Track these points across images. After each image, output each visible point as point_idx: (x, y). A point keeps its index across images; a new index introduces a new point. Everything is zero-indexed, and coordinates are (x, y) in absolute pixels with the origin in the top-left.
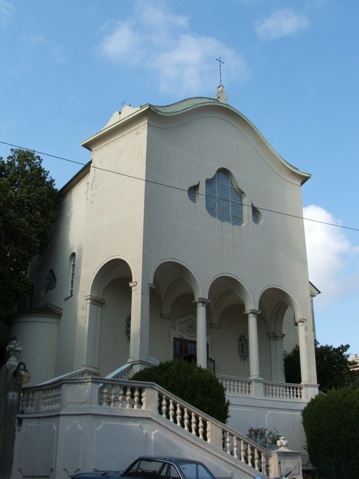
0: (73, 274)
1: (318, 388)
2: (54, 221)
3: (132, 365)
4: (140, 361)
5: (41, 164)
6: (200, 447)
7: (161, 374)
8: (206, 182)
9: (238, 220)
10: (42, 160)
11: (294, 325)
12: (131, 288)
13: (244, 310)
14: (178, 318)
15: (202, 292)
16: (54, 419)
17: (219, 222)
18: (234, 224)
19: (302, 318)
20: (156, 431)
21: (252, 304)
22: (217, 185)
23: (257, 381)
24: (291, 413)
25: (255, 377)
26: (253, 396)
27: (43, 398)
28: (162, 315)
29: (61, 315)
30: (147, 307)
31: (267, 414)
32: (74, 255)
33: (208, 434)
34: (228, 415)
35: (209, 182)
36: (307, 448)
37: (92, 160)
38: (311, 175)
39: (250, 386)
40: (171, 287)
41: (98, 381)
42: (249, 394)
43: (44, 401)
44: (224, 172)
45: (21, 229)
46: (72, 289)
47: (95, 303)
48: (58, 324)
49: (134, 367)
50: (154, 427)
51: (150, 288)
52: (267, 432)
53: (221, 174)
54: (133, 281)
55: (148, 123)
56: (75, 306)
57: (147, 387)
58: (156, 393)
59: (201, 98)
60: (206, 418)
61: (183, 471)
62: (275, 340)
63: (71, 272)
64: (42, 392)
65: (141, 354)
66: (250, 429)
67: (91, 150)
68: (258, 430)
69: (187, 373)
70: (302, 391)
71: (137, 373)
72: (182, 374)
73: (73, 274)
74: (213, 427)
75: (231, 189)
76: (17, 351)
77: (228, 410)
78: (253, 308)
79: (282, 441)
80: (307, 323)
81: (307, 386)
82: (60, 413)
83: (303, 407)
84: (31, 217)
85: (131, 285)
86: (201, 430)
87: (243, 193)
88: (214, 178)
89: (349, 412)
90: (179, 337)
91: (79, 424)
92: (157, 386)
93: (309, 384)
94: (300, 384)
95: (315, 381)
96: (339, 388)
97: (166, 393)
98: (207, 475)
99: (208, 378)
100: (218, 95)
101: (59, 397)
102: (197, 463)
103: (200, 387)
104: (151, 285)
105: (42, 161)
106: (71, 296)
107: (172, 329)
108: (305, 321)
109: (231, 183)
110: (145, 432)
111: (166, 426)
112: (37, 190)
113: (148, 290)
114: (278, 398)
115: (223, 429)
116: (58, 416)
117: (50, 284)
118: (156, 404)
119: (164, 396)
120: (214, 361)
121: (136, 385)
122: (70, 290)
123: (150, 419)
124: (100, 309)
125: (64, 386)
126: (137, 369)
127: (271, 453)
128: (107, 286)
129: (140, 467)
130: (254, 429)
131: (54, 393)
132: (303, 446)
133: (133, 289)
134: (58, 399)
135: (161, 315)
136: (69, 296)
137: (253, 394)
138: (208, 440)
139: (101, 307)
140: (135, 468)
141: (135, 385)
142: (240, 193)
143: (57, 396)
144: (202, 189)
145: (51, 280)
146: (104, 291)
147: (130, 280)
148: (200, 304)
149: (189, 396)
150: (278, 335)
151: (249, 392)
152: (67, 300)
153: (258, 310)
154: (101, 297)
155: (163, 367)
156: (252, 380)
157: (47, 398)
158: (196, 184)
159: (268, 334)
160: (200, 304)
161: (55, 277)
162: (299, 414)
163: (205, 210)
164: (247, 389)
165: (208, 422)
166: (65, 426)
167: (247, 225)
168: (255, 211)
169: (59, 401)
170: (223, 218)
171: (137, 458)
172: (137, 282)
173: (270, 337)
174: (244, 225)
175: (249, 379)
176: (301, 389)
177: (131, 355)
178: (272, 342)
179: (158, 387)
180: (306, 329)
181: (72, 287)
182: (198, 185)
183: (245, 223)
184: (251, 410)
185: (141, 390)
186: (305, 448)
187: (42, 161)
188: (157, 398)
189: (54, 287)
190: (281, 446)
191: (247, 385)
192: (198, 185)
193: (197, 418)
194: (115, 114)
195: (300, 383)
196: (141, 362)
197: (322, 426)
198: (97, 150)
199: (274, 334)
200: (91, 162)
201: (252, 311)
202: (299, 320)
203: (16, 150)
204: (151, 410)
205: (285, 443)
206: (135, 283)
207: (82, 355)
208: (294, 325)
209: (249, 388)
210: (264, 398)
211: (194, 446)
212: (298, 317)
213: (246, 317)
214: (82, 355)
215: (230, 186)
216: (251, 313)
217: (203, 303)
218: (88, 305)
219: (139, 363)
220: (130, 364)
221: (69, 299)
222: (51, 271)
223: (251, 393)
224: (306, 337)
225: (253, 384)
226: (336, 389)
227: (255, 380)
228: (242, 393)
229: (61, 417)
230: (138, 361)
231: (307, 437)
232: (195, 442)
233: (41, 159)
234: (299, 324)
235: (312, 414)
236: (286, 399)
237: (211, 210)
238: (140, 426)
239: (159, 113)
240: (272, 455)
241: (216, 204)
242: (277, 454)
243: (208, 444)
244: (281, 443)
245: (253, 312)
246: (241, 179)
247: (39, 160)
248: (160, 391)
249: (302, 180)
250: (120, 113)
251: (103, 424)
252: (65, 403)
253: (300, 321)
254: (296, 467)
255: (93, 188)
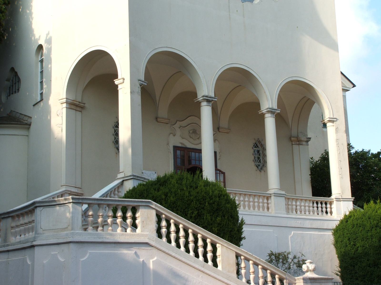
0: (42, 72)
1: (352, 202)
3: (123, 181)
4: (133, 176)
12: (117, 86)
15: (206, 87)
16: (28, 252)
19: (332, 117)
20: (155, 258)
21: (269, 101)
23: (277, 195)
24: (319, 233)
26: (273, 214)
27: (12, 228)
28: (158, 119)
29: (30, 125)
33: (218, 260)
34: (243, 236)
36: (339, 274)
39: (269, 201)
40: (167, 85)
41: (80, 201)
42: (268, 211)
43: (12, 230)
46: (41, 92)
47: (73, 107)
48: (27, 136)
49: (126, 183)
51: (140, 85)
52: (291, 256)
54: (119, 77)
56: (47, 111)
58: (154, 213)
62: (299, 144)
63: (39, 70)
64: (10, 220)
66: (270, 252)
68: (279, 254)
69: (191, 187)
71: (130, 190)
72: (185, 189)
73: (42, 72)
74: (225, 250)
77: (243, 230)
78: (271, 107)
79: (308, 264)
80: (338, 122)
81: (338, 200)
82: (35, 243)
83: (334, 225)
85: (116, 82)
86: (209, 255)
90: (180, 145)
91: (61, 255)
92: (154, 205)
95: (348, 194)
97: (166, 212)
99: (216, 192)
101: (33, 224)
103: (207, 204)
104: (143, 81)
106: (42, 100)
107: (171, 135)
108: (336, 121)
110: (141, 260)
111: (167, 251)
113: (139, 87)
115: (236, 252)
116: (33, 246)
117: (13, 86)
118: (154, 226)
120: (224, 173)
122: (39, 92)
123: (147, 244)
124: (79, 114)
125: (38, 210)
126: (129, 185)
128: (87, 86)
130: (274, 253)
131: (26, 219)
132: (335, 272)
133: (120, 87)
134: (31, 227)
135: (157, 118)
136: (39, 100)
137: (273, 211)
139: (81, 112)
141: (126, 204)
143: (30, 222)
147: (116, 76)
148: (204, 104)
149: (194, 215)
150: (302, 139)
151: (268, 209)
152: (36, 106)
153: (276, 108)
154: (79, 99)
155: (161, 182)
156: (271, 194)
157: (17, 226)
160: (204, 104)
164: (266, 205)
165: (218, 245)
166: (42, 258)
169: (32, 229)
172: (124, 79)
173: (292, 141)
176: (331, 203)
177: (121, 170)
178: (296, 147)
179: (156, 206)
180: (337, 130)
181: (42, 88)
184: (271, 230)
185: (134, 210)
186: (337, 275)
188: (154, 218)
189: (18, 90)
190: (307, 271)
191: (265, 201)
193: (204, 240)
196: (134, 177)
197: (358, 247)
199: (297, 137)
201: (269, 110)
202: (328, 119)
204: (148, 233)
206: (122, 80)
207: (60, 174)
209: (268, 204)
212: (327, 116)
213: (262, 117)
214: (60, 174)
216: (268, 112)
217: (208, 101)
218: (64, 110)
220: (121, 180)
222: (13, 69)
223: (270, 210)
224: (337, 140)
225: (273, 200)
226: (375, 203)
227: (274, 193)
229: (36, 249)
230: (130, 176)
232: (202, 269)
234: (328, 125)
235: (344, 233)
238: (136, 253)
240: (296, 282)
242: (302, 281)
244: (308, 267)
245: (271, 111)
251: (90, 253)
252: (40, 231)
253: (329, 121)
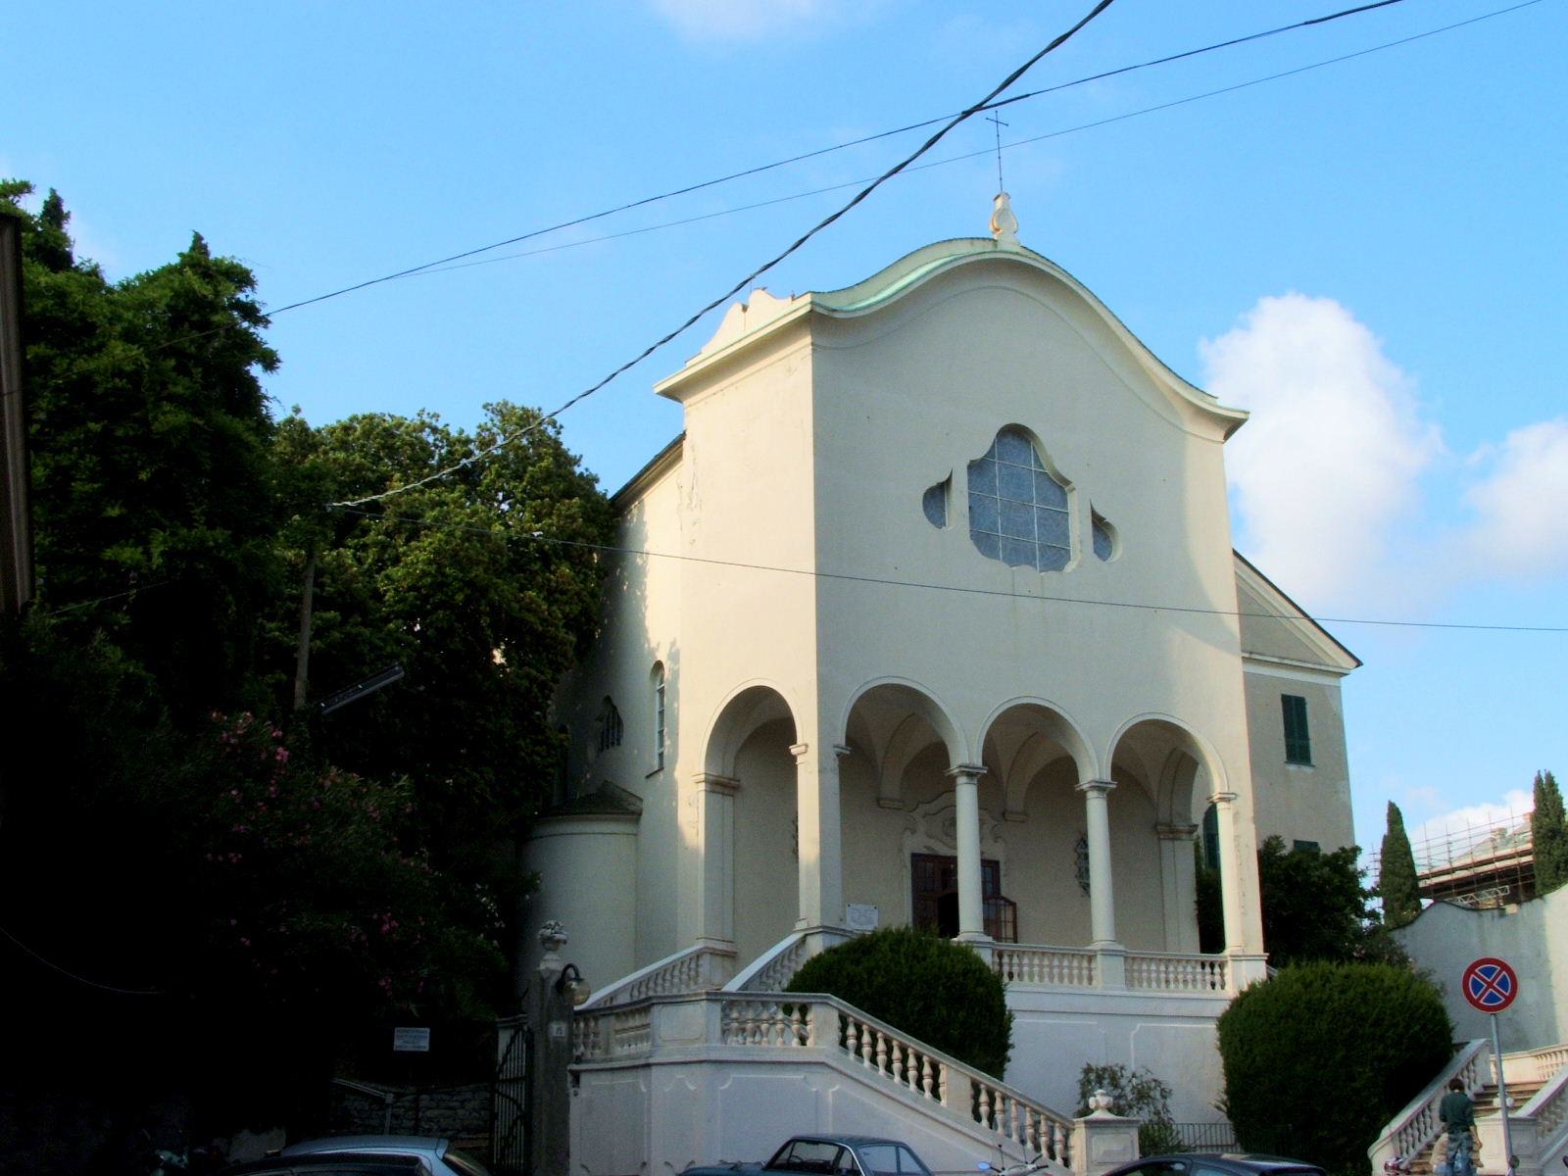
0: (661, 713)
1: (1264, 962)
2: (606, 575)
3: (806, 935)
4: (823, 927)
5: (560, 436)
6: (925, 1115)
7: (858, 962)
8: (970, 473)
9: (1055, 556)
10: (561, 427)
11: (1286, 762)
12: (794, 758)
13: (1076, 779)
14: (920, 806)
15: (966, 750)
16: (641, 1073)
17: (1005, 566)
18: (1046, 568)
19: (1226, 791)
20: (837, 1087)
21: (1094, 767)
22: (1000, 469)
23: (1108, 953)
24: (1195, 1026)
25: (1103, 943)
26: (1098, 991)
27: (617, 1032)
28: (881, 802)
29: (640, 814)
30: (836, 799)
31: (1134, 1029)
32: (659, 666)
33: (941, 1090)
34: (1010, 1042)
35: (976, 468)
36: (1223, 1106)
37: (684, 433)
38: (1249, 413)
39: (1093, 965)
40: (890, 747)
41: (719, 997)
42: (1090, 984)
43: (618, 1036)
44: (1016, 434)
45: (531, 618)
46: (661, 751)
47: (718, 789)
48: (635, 835)
49: (809, 939)
50: (834, 1079)
51: (838, 755)
52: (1127, 1074)
53: (1010, 440)
54: (799, 741)
55: (812, 344)
56: (672, 794)
57: (817, 1003)
58: (835, 1015)
59: (947, 244)
60: (937, 1058)
61: (865, 1158)
62: (1173, 839)
63: (657, 709)
64: (612, 1019)
65: (824, 910)
66: (1085, 1066)
67: (681, 402)
68: (1104, 1070)
69: (915, 957)
70: (1226, 971)
71: (813, 959)
72: (903, 961)
73: (661, 713)
74: (956, 1077)
75: (1037, 476)
76: (558, 941)
77: (1011, 1032)
78: (1097, 777)
79: (1098, 1098)
80: (1239, 802)
81: (1236, 958)
82: (651, 1061)
83: (1220, 1008)
84: (549, 580)
85: (794, 750)
86: (927, 1082)
87: (1067, 483)
88: (991, 453)
89: (1314, 1024)
90: (924, 851)
91: (691, 1081)
92: (835, 1000)
93: (1240, 953)
94: (1220, 955)
95: (1257, 945)
96: (1304, 963)
97: (855, 1013)
98: (916, 1169)
99: (959, 967)
100: (995, 224)
101: (648, 1030)
102: (898, 1145)
103: (941, 988)
104: (842, 748)
105: (562, 430)
106: (661, 769)
107: (908, 833)
108: (1235, 799)
109: (1037, 459)
110: (814, 1090)
111: (854, 1075)
112: (557, 510)
113: (835, 760)
114: (1163, 991)
115: (972, 1078)
116: (648, 1066)
117: (608, 730)
118: (836, 1035)
119: (851, 1019)
120: (1013, 905)
121: (796, 1000)
122: (657, 751)
123: (823, 1064)
124: (728, 801)
125: (655, 1010)
126: (816, 946)
127: (1074, 1124)
128: (744, 745)
129: (794, 1154)
130: (1094, 1068)
131: (637, 1021)
132: (1213, 1102)
133: (799, 760)
134: (645, 1033)
135: (878, 800)
136: (656, 768)
137: (1098, 984)
138: (943, 1101)
139: (732, 796)
140: (785, 1156)
141: (791, 1000)
142: (1061, 485)
143: (644, 1026)
144: (959, 500)
145: (611, 727)
146: (737, 758)
147: (792, 739)
148: (962, 780)
149: (917, 1009)
150: (1181, 828)
151: (1090, 979)
152: (651, 778)
153: (1109, 779)
154: (729, 773)
155: (862, 948)
156: (1095, 951)
157: (624, 1030)
158: (944, 478)
159: (1155, 827)
160: (962, 780)
161: (619, 717)
162: (1212, 1026)
163: (969, 544)
164: (1085, 972)
165: (941, 1066)
166: (663, 1085)
167: (1080, 566)
168: (1100, 526)
169: (646, 1038)
170: (1018, 555)
171: (789, 1139)
172: (807, 746)
173: (1158, 833)
174: (1070, 567)
175: (1089, 948)
176: (1222, 966)
177: (802, 915)
178: (1166, 845)
179: (838, 1002)
180: (1236, 816)
181: (662, 744)
182: (948, 481)
183: (1075, 560)
184: (1093, 1022)
185: (804, 1010)
186: (1218, 1108)
187: (562, 430)
188: (836, 1023)
189: (618, 740)
190: (1097, 1108)
191: (1085, 964)
192: (948, 481)
193: (919, 1058)
194: (732, 309)
195: (1222, 952)
196: (826, 930)
197: (1256, 1056)
198: (695, 404)
199: (1170, 825)
200: (683, 437)
201: (1093, 784)
202: (1219, 796)
203: (494, 406)
204: (825, 1047)
205: (1105, 1103)
206: (803, 748)
207: (694, 925)
208: (1286, 762)
209: (1090, 970)
210: (1126, 993)
211: (913, 1114)
212: (1218, 788)
213: (1082, 797)
214: (694, 925)
215: (1000, 534)
216: (1093, 788)
217: (970, 775)
218: (702, 796)
219: (821, 932)
220: (801, 935)
221: (656, 776)
222: (608, 699)
223: (1094, 982)
224: (1237, 837)
225: (1099, 962)
226: (1298, 966)
227: (1102, 950)
228: (1071, 982)
229: (654, 1069)
230: (818, 927)
231: (1230, 1082)
232: (914, 1105)
233: (558, 425)
234: (1221, 806)
235: (1245, 1028)
236: (1194, 993)
237: (983, 540)
238: (805, 1078)
239: (837, 315)
240: (1077, 1126)
241: (995, 524)
242: (1083, 1125)
243: (942, 1108)
244: (1097, 1101)
245: (1099, 787)
246: (1059, 448)
247: (555, 427)
248: (842, 1008)
249: (1226, 429)
250: (745, 309)
251: (734, 1078)
252: (659, 1042)
253: (1222, 799)
254: (1125, 1149)
255: (693, 505)
